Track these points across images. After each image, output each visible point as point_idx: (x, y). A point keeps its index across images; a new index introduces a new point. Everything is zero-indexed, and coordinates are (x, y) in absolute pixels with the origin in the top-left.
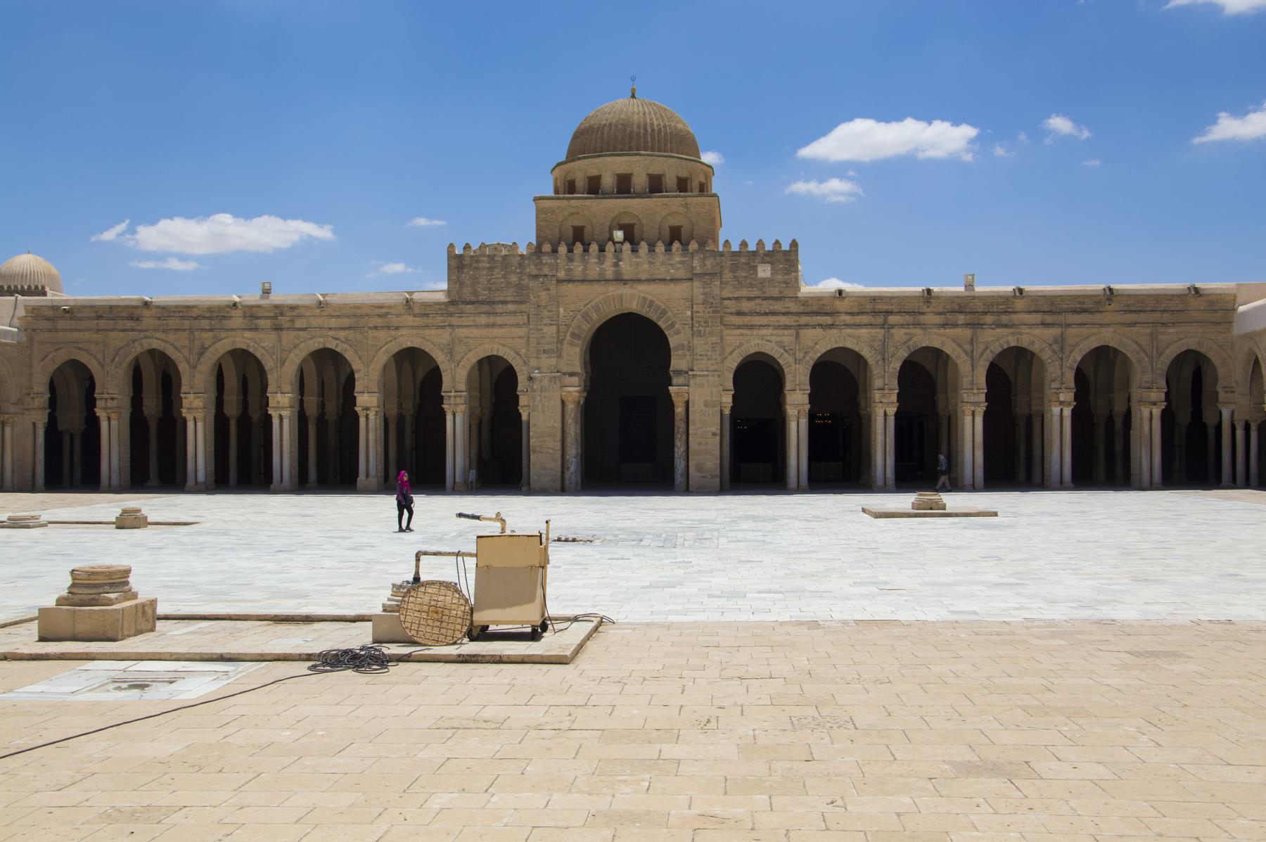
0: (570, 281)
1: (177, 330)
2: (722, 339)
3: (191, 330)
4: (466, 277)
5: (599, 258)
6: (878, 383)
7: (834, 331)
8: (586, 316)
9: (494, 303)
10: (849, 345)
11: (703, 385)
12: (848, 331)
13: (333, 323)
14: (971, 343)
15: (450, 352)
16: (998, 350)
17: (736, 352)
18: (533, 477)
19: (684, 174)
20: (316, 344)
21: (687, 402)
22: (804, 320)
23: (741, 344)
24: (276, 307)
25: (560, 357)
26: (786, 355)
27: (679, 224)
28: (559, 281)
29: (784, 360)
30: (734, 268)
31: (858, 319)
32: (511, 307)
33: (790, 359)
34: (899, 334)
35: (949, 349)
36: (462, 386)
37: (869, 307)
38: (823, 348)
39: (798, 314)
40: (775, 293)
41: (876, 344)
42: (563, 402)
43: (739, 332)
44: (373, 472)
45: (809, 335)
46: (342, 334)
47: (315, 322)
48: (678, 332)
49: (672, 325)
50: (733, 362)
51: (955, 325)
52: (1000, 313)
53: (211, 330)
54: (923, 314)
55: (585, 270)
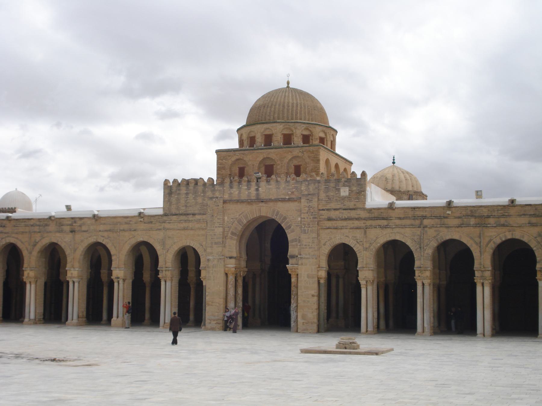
0: (230, 201)
1: (23, 233)
2: (318, 235)
3: (30, 232)
4: (174, 199)
5: (247, 186)
6: (417, 263)
7: (389, 230)
8: (240, 221)
9: (188, 214)
10: (398, 238)
13: (102, 228)
14: (480, 237)
15: (163, 243)
16: (498, 241)
17: (328, 243)
18: (207, 321)
19: (306, 133)
20: (92, 240)
21: (298, 275)
22: (369, 223)
23: (331, 239)
24: (72, 218)
25: (224, 247)
26: (358, 245)
27: (300, 164)
28: (225, 202)
29: (357, 248)
30: (327, 190)
31: (404, 222)
32: (198, 217)
33: (361, 248)
34: (431, 232)
35: (465, 240)
36: (169, 264)
37: (411, 214)
38: (382, 240)
39: (365, 219)
40: (351, 205)
41: (416, 238)
42: (226, 274)
43: (329, 230)
44: (121, 315)
45: (373, 233)
46: (105, 234)
47: (92, 228)
48: (293, 231)
49: (289, 227)
50: (326, 250)
51: (468, 225)
52: (499, 217)
53: (39, 232)
54: (446, 218)
55: (240, 193)
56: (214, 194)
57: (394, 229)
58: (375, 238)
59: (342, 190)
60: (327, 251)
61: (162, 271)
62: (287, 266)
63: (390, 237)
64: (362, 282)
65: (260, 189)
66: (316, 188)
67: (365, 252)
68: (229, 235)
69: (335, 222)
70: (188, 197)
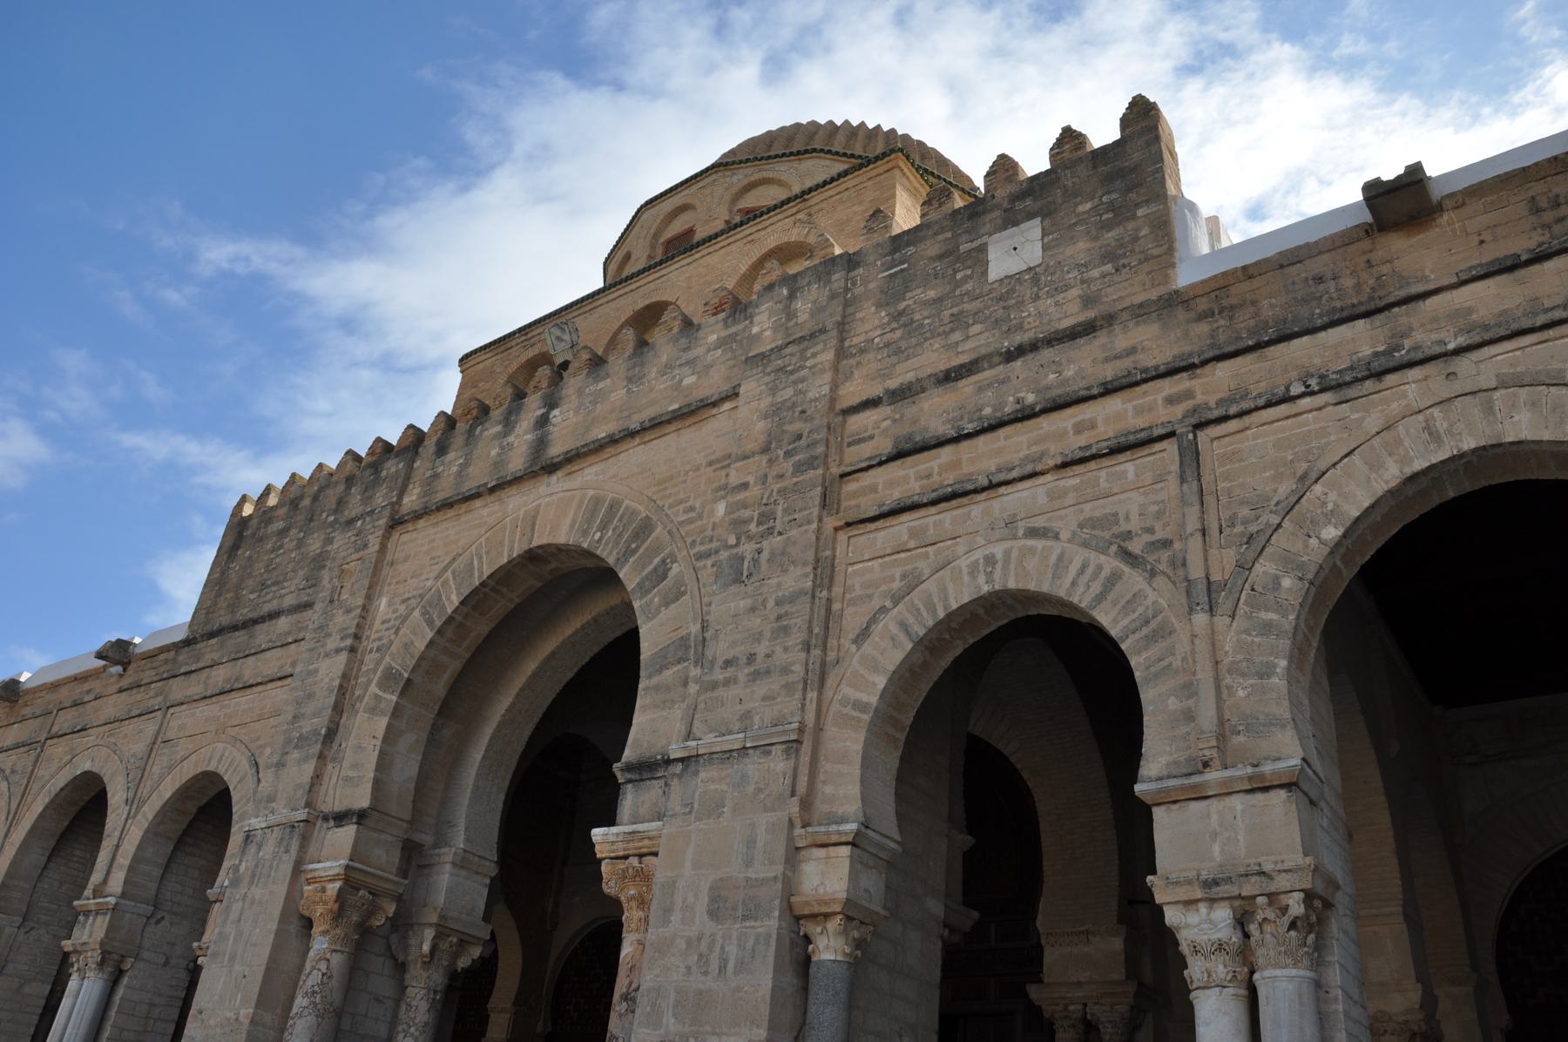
2: (825, 571)
7: (1412, 387)
9: (255, 622)
11: (714, 808)
12: (1502, 358)
17: (888, 623)
22: (1219, 380)
23: (913, 582)
26: (1134, 580)
33: (1159, 595)
43: (901, 528)
49: (661, 574)
50: (871, 669)
56: (367, 500)
57: (1464, 364)
58: (1285, 488)
59: (992, 255)
60: (881, 682)
61: (87, 913)
62: (597, 833)
63: (1434, 436)
64: (1199, 926)
65: (556, 412)
66: (833, 297)
67: (1201, 619)
68: (373, 689)
69: (946, 453)
70: (281, 547)
